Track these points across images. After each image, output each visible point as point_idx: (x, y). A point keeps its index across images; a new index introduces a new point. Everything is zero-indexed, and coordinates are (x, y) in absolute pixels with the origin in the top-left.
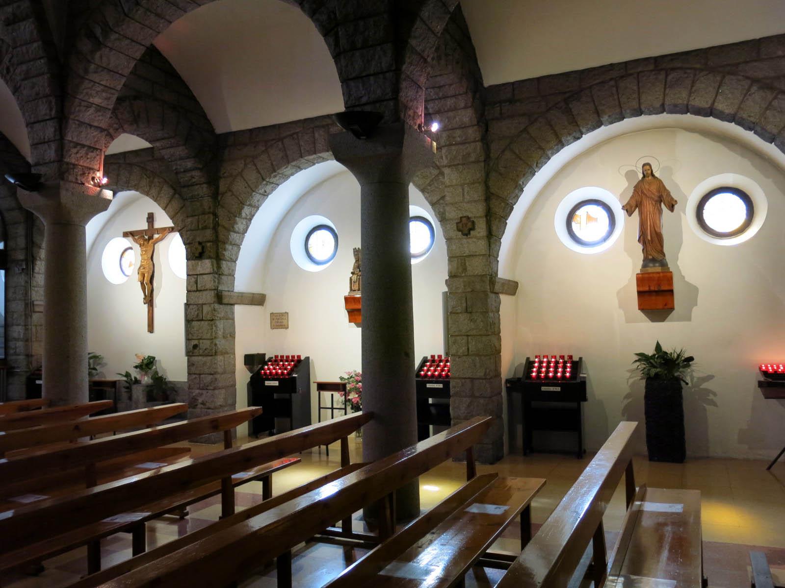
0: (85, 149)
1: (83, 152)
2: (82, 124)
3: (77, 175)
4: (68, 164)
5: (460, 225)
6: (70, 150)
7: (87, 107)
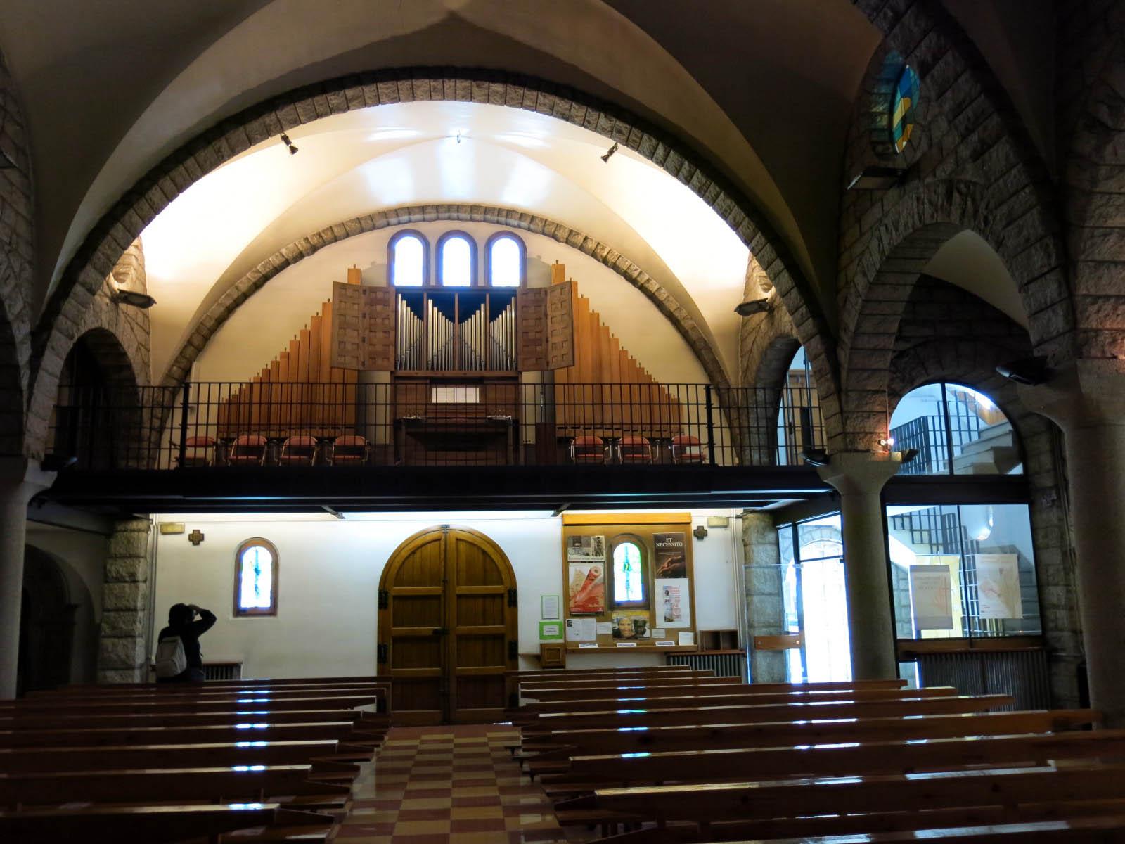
0: (1112, 300)
1: (1108, 307)
2: (1100, 263)
3: (1103, 346)
4: (1086, 331)
6: (1086, 310)
7: (1105, 235)
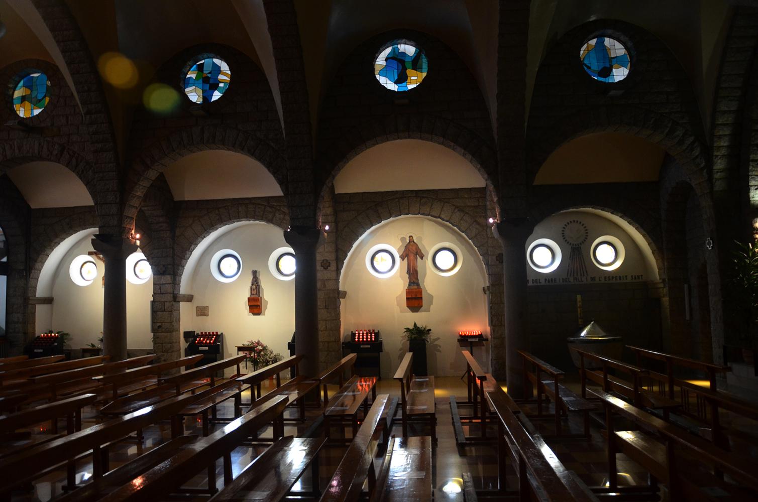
5: (323, 264)
6: (124, 220)
